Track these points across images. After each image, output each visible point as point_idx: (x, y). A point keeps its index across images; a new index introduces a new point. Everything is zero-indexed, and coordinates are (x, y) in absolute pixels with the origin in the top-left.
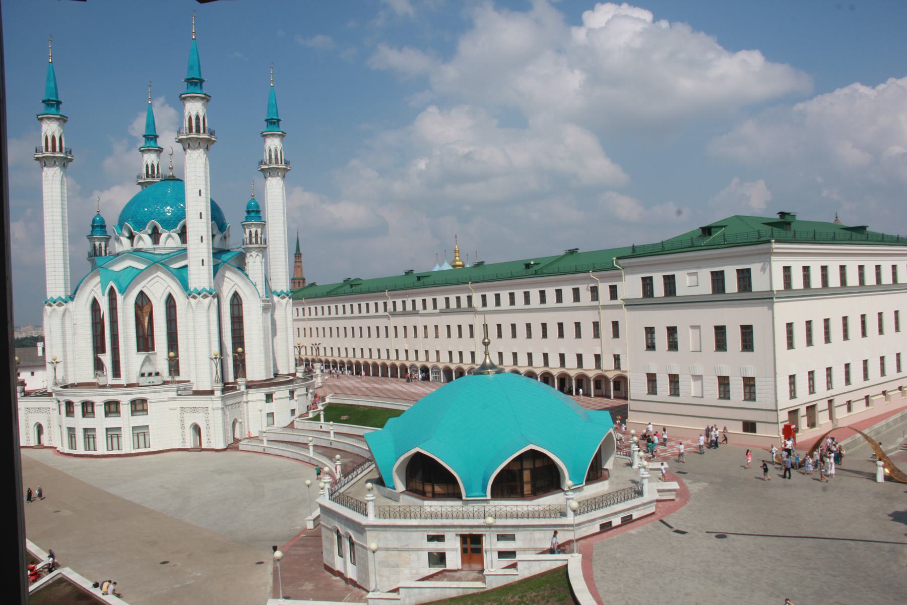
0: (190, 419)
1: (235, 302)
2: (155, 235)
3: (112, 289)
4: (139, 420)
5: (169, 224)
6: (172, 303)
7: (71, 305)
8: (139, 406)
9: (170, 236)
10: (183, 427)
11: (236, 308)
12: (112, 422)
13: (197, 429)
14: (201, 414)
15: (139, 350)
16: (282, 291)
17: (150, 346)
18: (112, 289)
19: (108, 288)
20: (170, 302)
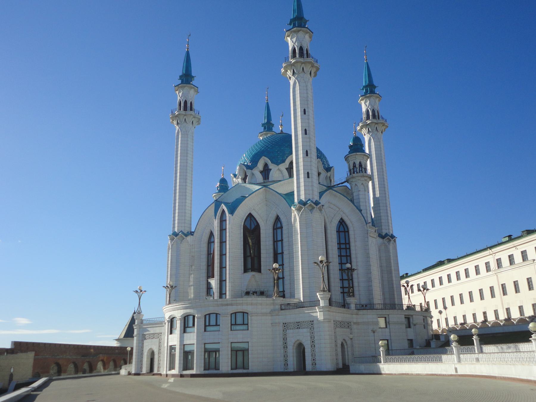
0: (294, 336)
1: (342, 229)
3: (223, 211)
4: (239, 336)
5: (278, 161)
6: (279, 225)
7: (189, 238)
8: (240, 320)
10: (285, 347)
11: (342, 234)
12: (211, 336)
13: (301, 349)
14: (305, 330)
15: (246, 270)
16: (386, 235)
17: (256, 266)
20: (277, 224)
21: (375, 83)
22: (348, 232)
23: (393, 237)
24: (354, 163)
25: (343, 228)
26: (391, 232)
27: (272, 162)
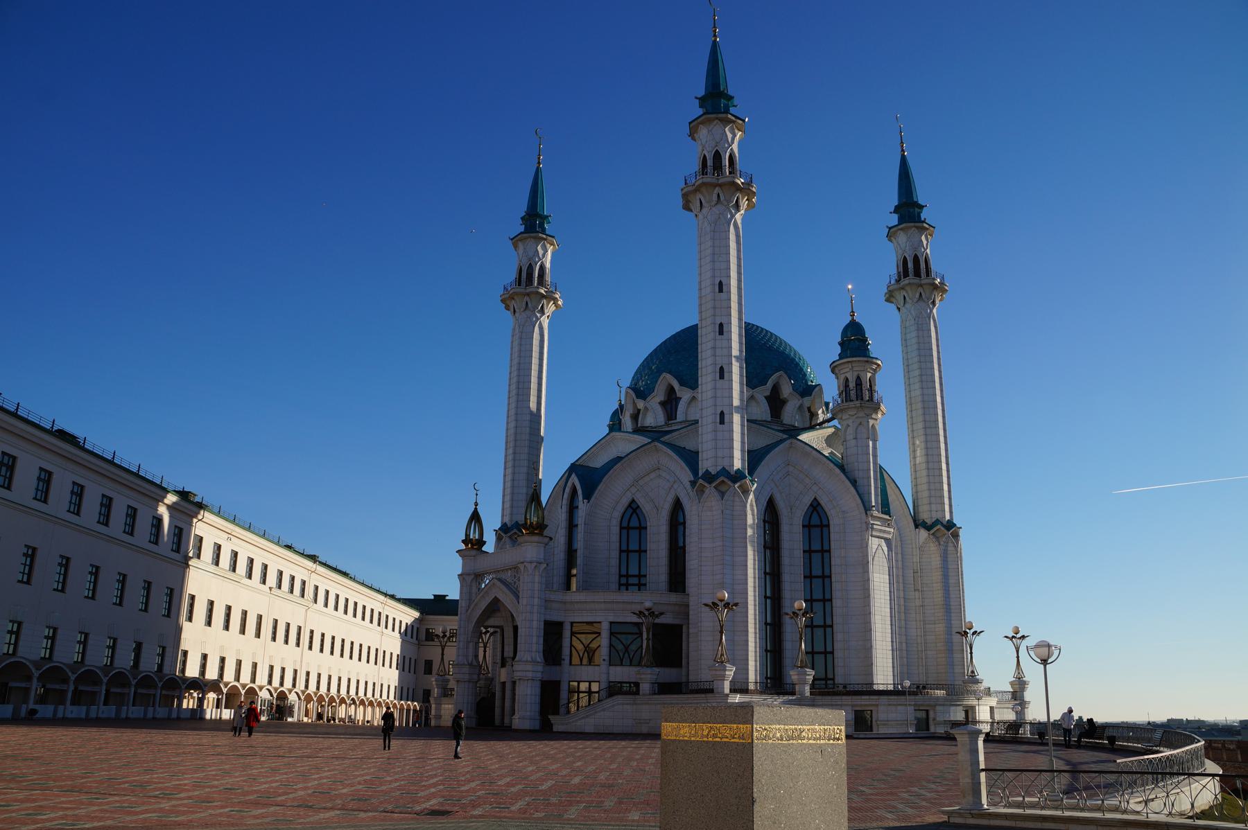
2: (670, 404)
3: (574, 490)
9: (694, 398)
16: (937, 522)
18: (574, 490)
19: (567, 490)
21: (921, 196)
22: (828, 526)
23: (950, 525)
24: (847, 379)
25: (817, 521)
26: (948, 517)
27: (682, 383)
